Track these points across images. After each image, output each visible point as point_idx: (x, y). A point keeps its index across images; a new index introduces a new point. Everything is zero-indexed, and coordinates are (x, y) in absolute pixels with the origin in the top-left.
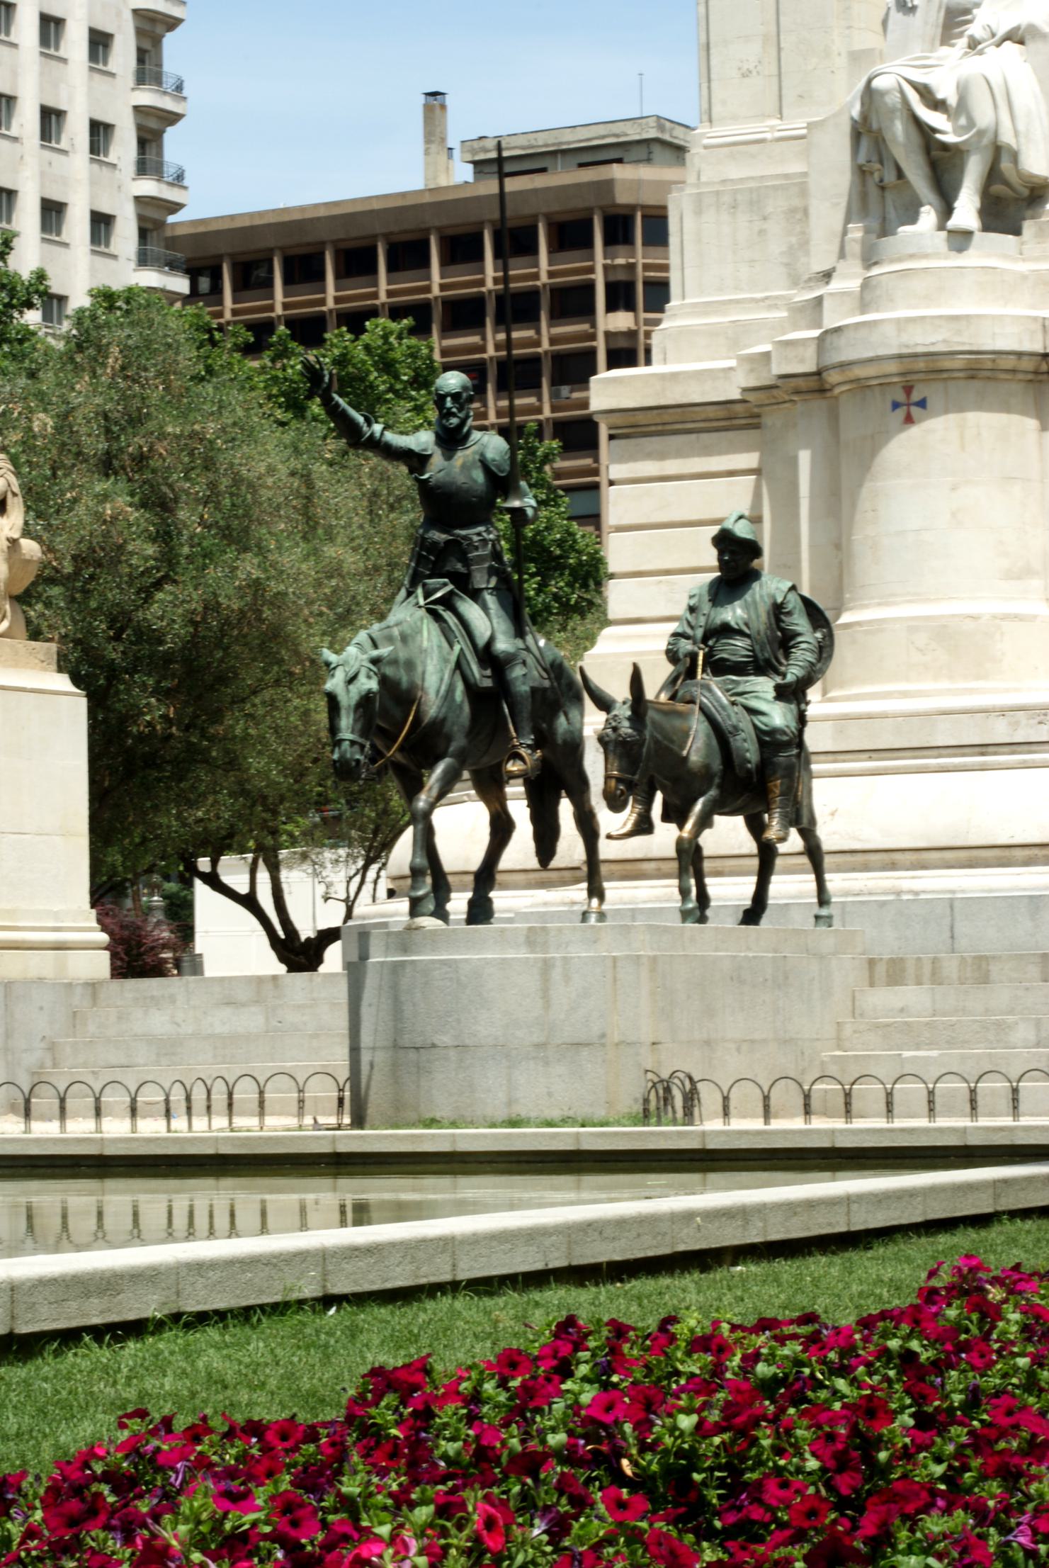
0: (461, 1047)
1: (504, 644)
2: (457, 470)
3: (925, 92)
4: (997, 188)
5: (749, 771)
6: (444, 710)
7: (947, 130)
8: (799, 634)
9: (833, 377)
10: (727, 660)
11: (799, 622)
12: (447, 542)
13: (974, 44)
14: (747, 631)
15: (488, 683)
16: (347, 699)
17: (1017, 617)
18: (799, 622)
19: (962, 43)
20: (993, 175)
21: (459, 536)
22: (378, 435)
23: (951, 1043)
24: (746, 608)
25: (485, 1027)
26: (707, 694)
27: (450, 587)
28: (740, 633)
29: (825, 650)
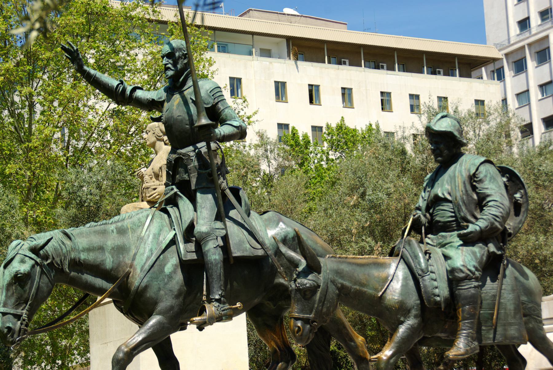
2: (175, 108)
5: (438, 303)
6: (145, 280)
8: (488, 196)
10: (439, 222)
14: (449, 197)
15: (194, 256)
21: (180, 154)
22: (128, 92)
26: (407, 247)
27: (176, 190)
28: (446, 200)
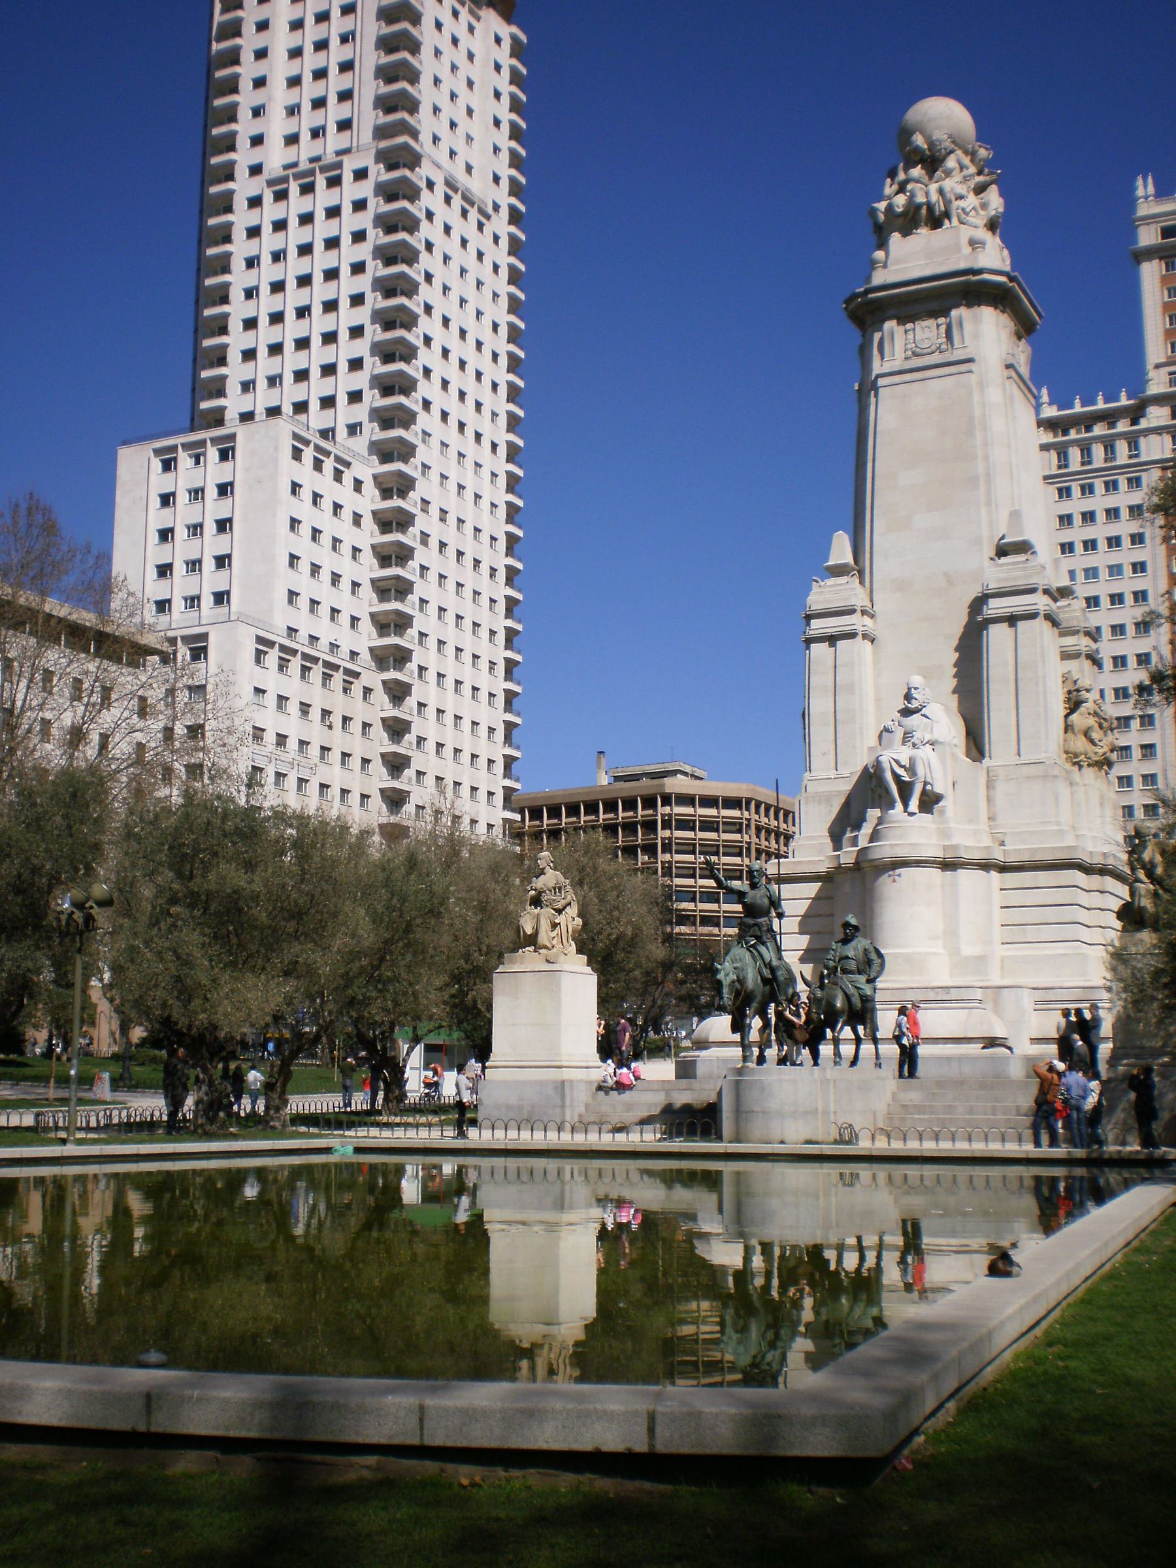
0: (764, 1112)
1: (775, 963)
3: (897, 762)
4: (925, 798)
7: (906, 778)
9: (865, 865)
11: (873, 956)
12: (755, 925)
13: (914, 745)
16: (726, 983)
17: (934, 954)
18: (873, 956)
19: (910, 744)
20: (924, 792)
23: (932, 1113)
24: (855, 949)
25: (773, 1105)
29: (882, 965)
